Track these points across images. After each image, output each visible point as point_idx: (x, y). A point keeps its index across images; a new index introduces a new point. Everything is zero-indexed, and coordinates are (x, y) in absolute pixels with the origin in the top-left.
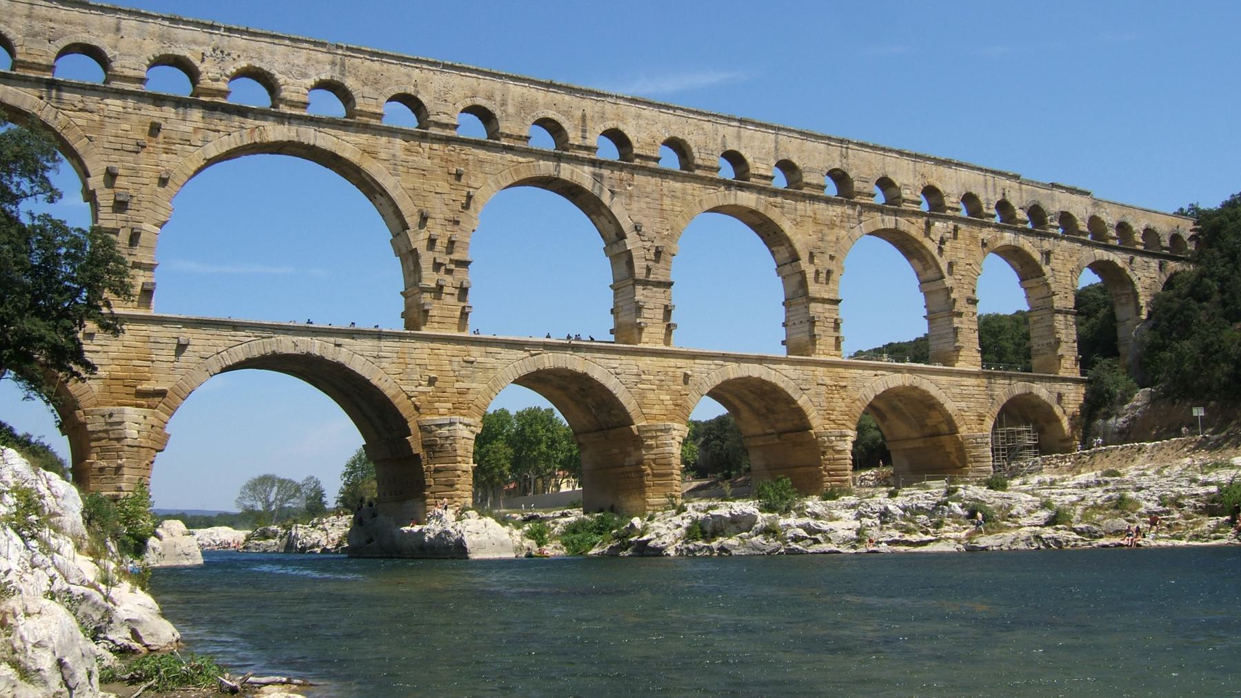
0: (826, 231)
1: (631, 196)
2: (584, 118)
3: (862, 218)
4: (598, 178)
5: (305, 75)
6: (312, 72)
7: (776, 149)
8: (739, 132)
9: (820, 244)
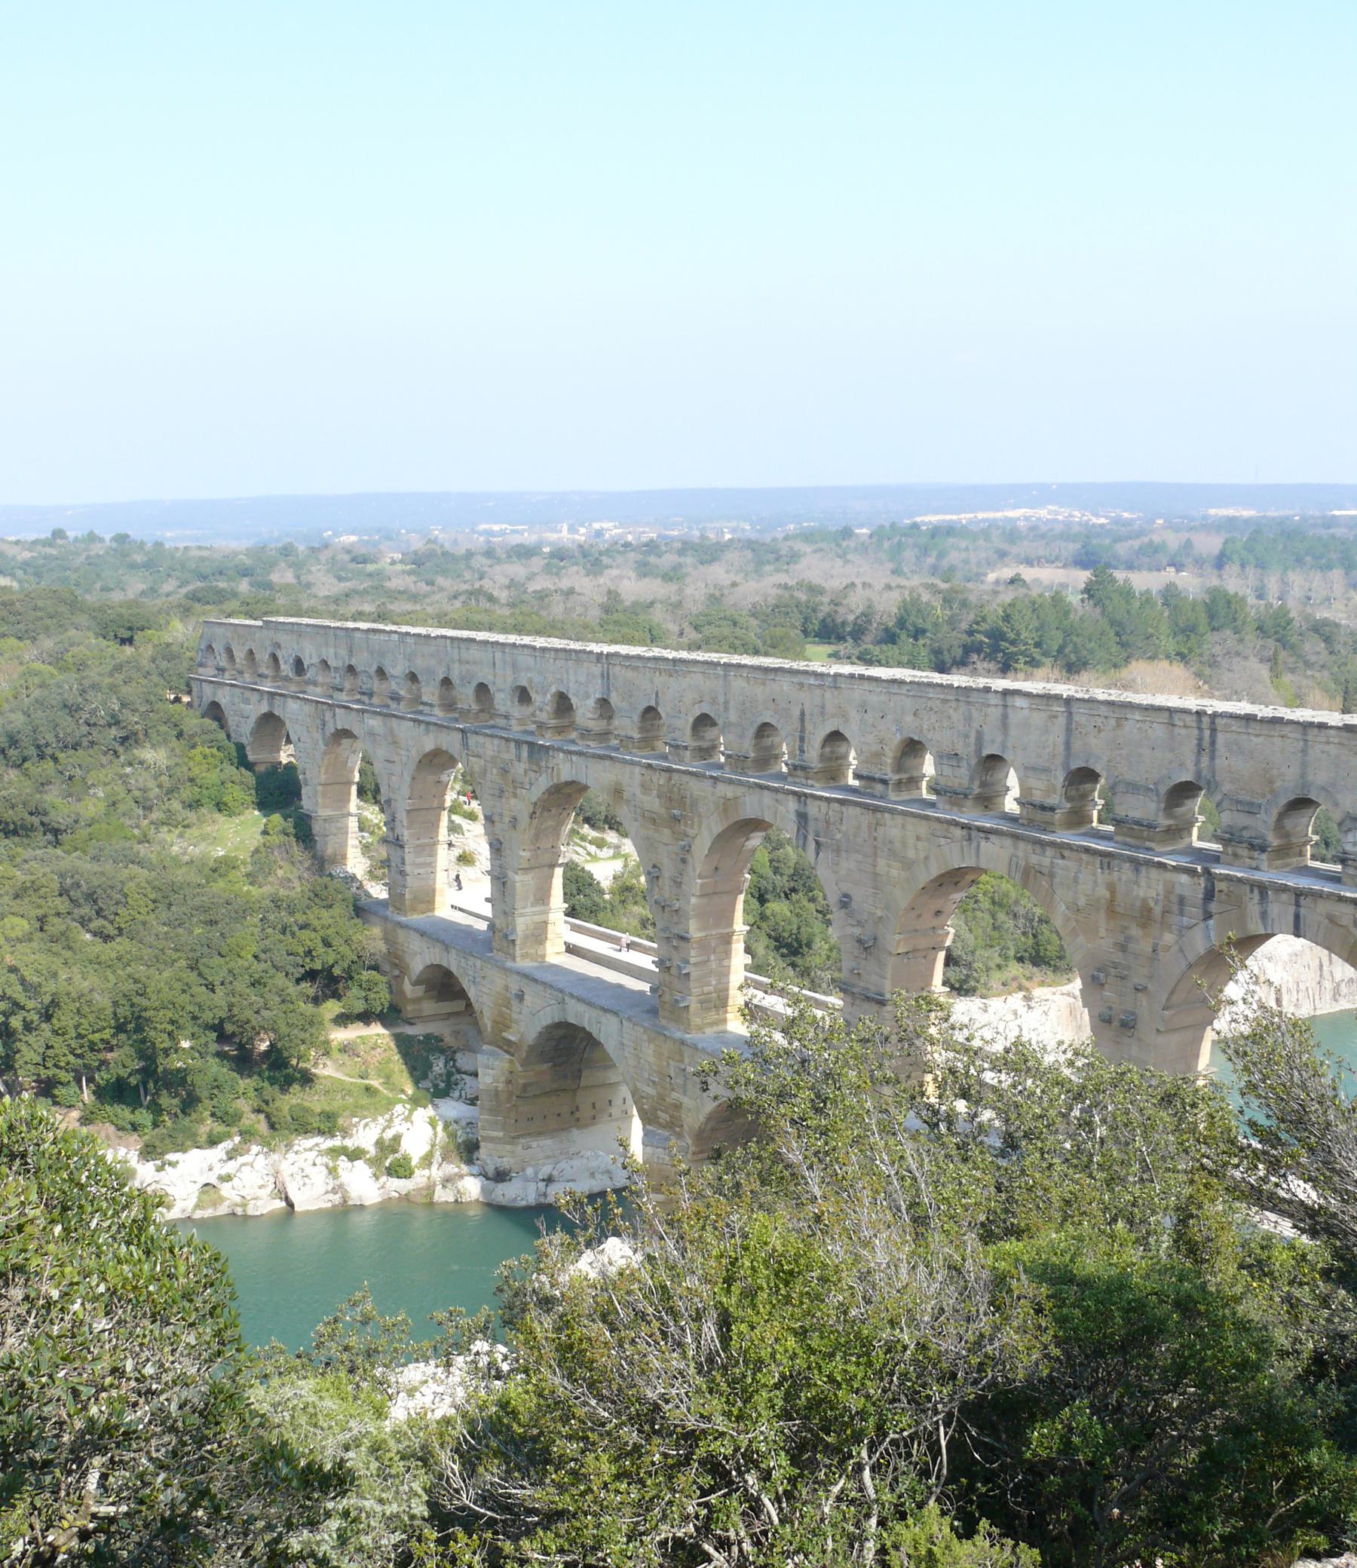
0: (1135, 931)
1: (838, 851)
2: (803, 714)
3: (1213, 907)
4: (802, 817)
5: (587, 696)
6: (591, 690)
7: (1068, 745)
8: (1005, 717)
9: (1118, 957)
